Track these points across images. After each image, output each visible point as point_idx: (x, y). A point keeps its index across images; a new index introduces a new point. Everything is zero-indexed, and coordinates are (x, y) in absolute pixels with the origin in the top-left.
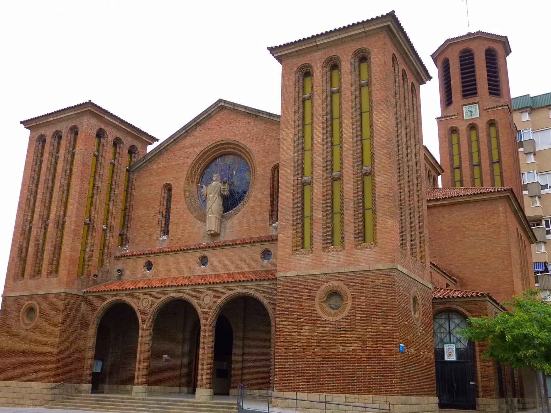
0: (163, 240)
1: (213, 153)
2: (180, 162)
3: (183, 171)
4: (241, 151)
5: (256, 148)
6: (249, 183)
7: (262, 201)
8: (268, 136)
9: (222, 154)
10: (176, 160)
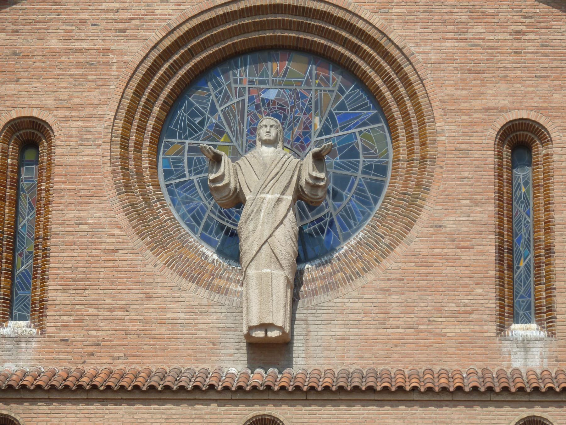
0: (17, 339)
1: (232, 33)
2: (84, 44)
3: (105, 81)
4: (356, 49)
5: (428, 48)
6: (381, 169)
7: (463, 244)
8: (475, 15)
9: (268, 43)
10: (68, 34)
